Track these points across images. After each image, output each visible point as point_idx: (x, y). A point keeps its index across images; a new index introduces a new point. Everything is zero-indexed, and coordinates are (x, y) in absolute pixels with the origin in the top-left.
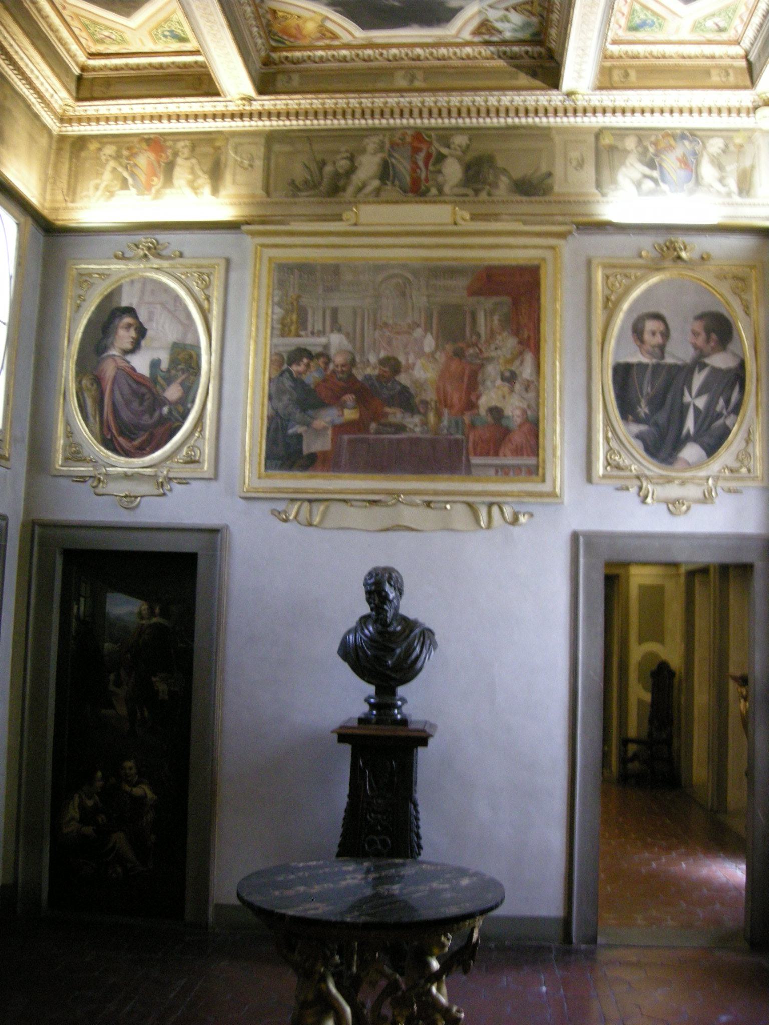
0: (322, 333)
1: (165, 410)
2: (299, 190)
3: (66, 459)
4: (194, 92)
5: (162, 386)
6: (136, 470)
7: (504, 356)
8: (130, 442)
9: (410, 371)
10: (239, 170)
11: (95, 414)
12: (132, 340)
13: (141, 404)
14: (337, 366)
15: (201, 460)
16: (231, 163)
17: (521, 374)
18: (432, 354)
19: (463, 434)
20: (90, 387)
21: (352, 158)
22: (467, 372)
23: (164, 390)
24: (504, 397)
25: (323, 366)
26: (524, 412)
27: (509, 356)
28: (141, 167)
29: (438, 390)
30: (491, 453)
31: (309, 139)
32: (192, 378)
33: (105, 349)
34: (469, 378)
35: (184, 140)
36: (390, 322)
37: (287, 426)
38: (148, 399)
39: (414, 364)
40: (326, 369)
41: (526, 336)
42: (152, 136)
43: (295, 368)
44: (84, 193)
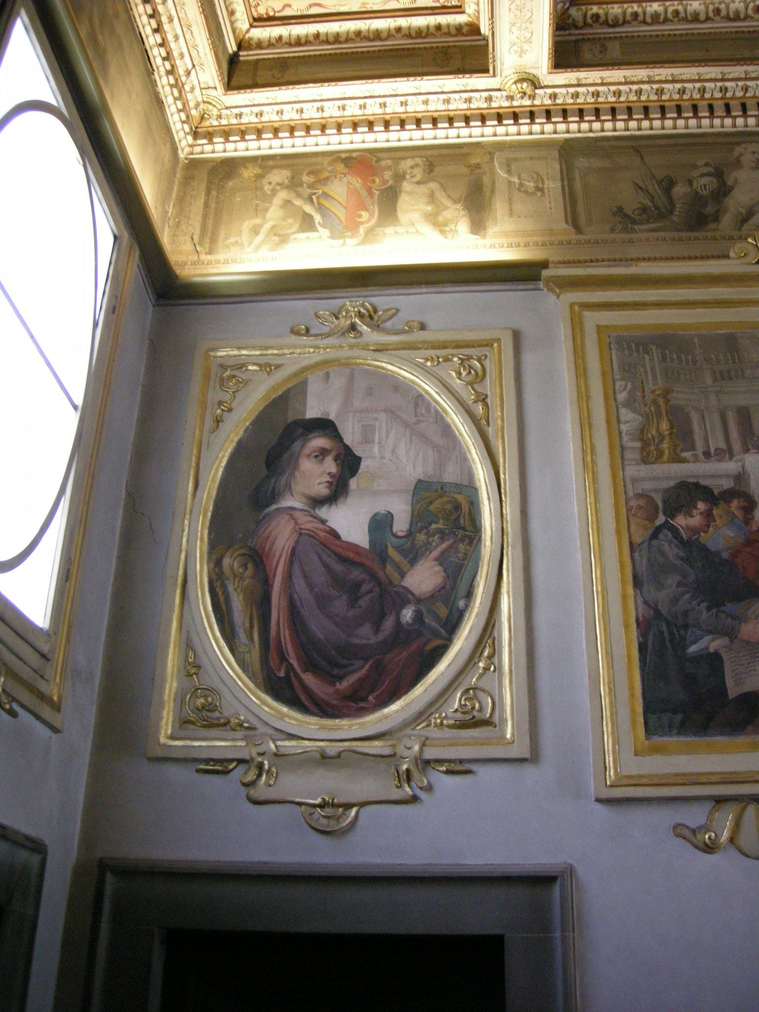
0: (727, 453)
1: (408, 614)
2: (634, 222)
3: (183, 723)
4: (439, 70)
5: (397, 566)
6: (346, 744)
8: (333, 684)
10: (517, 196)
11: (251, 627)
12: (328, 479)
13: (353, 603)
15: (496, 719)
16: (501, 186)
20: (241, 570)
21: (719, 174)
23: (403, 575)
25: (739, 514)
28: (336, 197)
31: (638, 151)
32: (462, 547)
33: (274, 496)
35: (413, 157)
37: (683, 639)
38: (371, 591)
42: (354, 155)
43: (681, 521)
44: (232, 240)
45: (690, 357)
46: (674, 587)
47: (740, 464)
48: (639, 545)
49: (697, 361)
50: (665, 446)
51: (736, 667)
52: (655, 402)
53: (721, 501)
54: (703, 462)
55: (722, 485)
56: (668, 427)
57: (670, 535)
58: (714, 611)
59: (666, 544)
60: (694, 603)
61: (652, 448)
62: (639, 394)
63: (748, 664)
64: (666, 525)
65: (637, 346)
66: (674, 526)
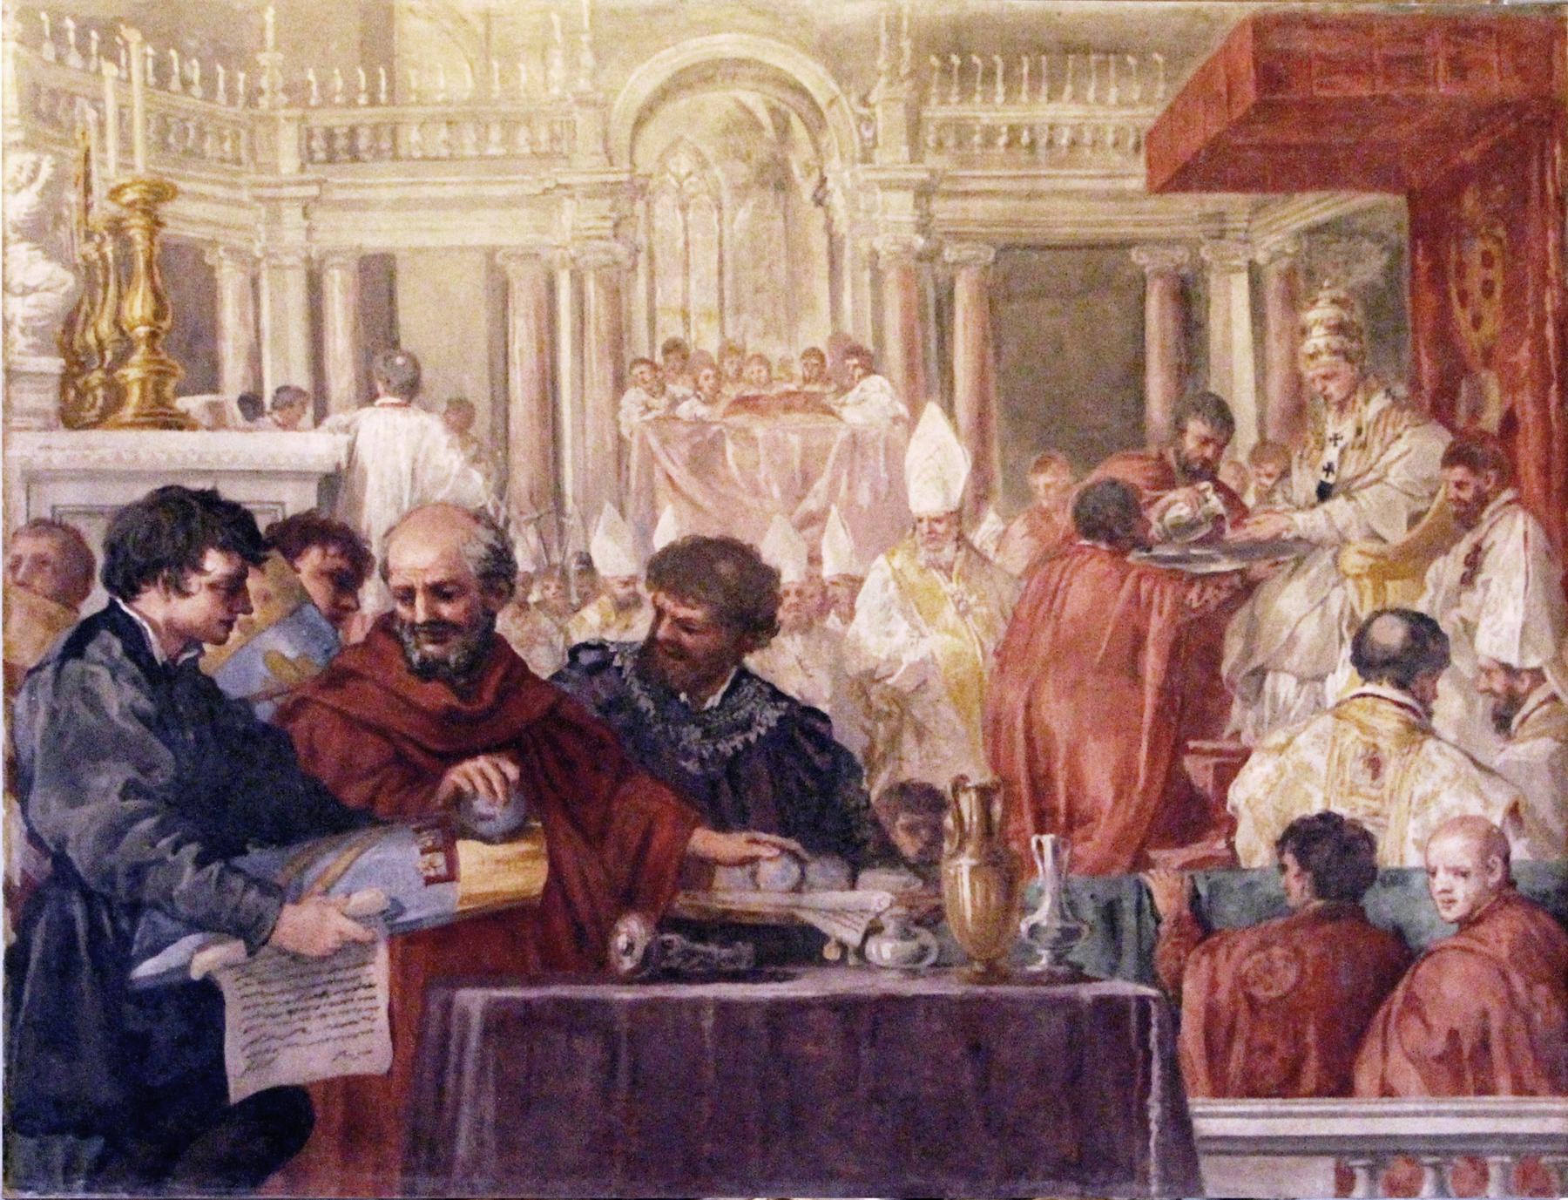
7: (1375, 536)
9: (832, 621)
14: (407, 595)
17: (1469, 628)
18: (959, 521)
19: (1146, 973)
22: (1156, 625)
24: (1375, 765)
25: (319, 592)
26: (1494, 844)
27: (1398, 534)
29: (995, 728)
30: (1311, 1074)
34: (1175, 654)
36: (707, 340)
37: (125, 940)
39: (855, 583)
40: (339, 615)
41: (1491, 419)
45: (242, 76)
46: (114, 797)
47: (343, 439)
48: (31, 672)
49: (261, 92)
50: (133, 373)
51: (256, 1022)
52: (117, 228)
53: (275, 554)
54: (237, 429)
55: (282, 504)
56: (148, 313)
57: (117, 646)
58: (215, 868)
59: (105, 675)
60: (164, 842)
61: (96, 377)
62: (73, 196)
63: (290, 1012)
64: (111, 619)
65: (83, 34)
66: (130, 620)
